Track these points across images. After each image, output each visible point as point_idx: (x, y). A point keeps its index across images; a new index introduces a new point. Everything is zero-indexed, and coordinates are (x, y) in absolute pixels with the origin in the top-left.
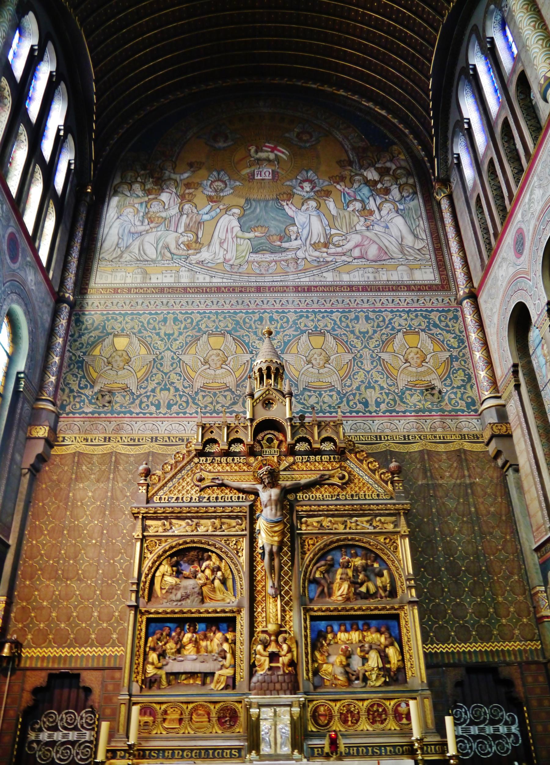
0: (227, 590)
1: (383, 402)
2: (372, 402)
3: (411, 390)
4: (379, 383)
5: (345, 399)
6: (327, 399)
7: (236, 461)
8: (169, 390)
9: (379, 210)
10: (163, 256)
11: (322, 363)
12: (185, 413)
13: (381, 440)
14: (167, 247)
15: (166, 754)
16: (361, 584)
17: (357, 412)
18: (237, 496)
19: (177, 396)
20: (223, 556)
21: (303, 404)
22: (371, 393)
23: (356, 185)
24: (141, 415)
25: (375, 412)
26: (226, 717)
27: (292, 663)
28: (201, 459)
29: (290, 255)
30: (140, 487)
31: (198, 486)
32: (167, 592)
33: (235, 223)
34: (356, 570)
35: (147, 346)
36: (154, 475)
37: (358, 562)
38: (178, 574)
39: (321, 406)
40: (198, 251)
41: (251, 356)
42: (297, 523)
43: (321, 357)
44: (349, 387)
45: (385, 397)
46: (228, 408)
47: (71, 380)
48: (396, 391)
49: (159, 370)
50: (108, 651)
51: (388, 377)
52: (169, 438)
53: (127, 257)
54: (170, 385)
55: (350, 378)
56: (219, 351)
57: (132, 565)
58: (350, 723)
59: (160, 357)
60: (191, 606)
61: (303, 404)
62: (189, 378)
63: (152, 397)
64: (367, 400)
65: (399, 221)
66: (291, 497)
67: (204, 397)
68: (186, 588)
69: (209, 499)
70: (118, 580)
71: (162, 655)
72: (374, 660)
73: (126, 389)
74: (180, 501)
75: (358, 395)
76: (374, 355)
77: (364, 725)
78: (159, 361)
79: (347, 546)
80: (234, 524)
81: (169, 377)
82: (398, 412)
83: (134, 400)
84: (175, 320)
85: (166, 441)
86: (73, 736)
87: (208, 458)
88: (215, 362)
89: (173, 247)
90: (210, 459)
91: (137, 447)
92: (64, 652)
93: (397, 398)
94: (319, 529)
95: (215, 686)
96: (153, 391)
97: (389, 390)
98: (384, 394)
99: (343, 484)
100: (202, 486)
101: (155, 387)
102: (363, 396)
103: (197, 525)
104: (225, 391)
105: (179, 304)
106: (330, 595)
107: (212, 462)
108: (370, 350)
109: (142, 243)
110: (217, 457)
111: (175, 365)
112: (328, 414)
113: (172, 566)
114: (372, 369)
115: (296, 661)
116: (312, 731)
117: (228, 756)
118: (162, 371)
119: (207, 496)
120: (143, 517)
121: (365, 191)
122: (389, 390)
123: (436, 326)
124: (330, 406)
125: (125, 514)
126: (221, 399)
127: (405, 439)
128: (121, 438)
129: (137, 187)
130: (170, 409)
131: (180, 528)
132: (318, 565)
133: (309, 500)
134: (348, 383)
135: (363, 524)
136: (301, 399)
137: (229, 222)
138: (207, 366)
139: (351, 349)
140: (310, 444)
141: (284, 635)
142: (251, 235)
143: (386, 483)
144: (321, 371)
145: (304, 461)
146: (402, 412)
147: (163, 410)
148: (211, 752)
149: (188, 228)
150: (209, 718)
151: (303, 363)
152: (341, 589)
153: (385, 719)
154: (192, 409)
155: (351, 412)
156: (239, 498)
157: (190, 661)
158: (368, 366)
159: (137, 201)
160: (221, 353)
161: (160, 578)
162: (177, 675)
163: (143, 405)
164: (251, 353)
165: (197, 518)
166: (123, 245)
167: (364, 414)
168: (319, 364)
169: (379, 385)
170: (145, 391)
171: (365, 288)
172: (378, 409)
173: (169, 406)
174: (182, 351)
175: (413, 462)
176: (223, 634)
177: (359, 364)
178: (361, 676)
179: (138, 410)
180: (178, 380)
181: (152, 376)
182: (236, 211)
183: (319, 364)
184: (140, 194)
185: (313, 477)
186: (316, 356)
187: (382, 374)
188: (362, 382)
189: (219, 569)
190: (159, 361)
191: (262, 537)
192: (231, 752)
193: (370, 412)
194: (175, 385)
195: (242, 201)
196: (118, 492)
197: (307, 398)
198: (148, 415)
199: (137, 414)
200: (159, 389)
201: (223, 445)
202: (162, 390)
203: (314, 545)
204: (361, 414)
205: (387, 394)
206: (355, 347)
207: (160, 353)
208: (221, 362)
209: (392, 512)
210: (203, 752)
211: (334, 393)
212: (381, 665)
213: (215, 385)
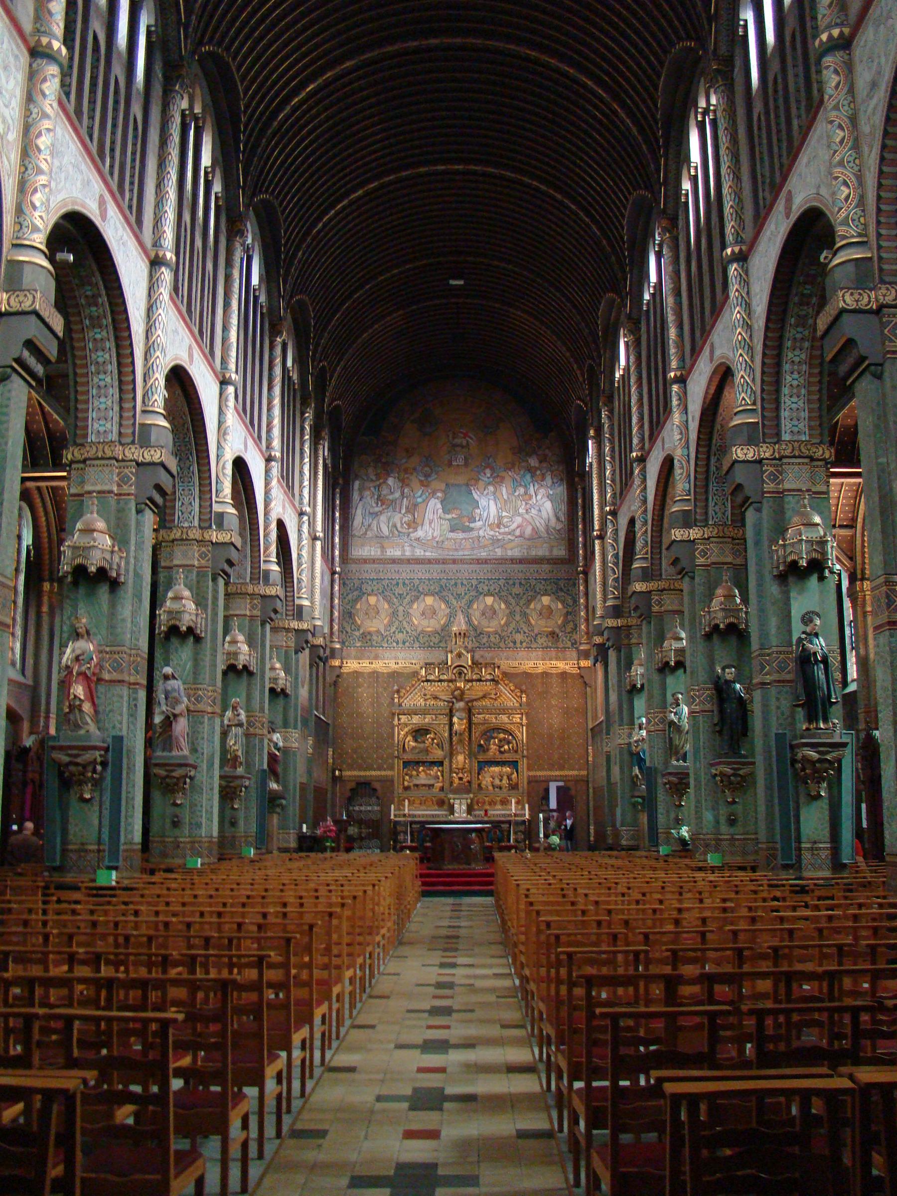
2: (518, 642)
10: (391, 532)
14: (395, 526)
29: (475, 533)
33: (439, 506)
35: (389, 602)
37: (502, 736)
38: (416, 741)
47: (345, 625)
50: (383, 773)
53: (370, 534)
60: (423, 757)
65: (548, 505)
71: (411, 776)
72: (505, 781)
73: (378, 632)
77: (499, 807)
79: (497, 729)
84: (404, 584)
86: (369, 808)
89: (399, 525)
92: (362, 773)
95: (435, 790)
105: (405, 572)
106: (488, 750)
109: (378, 523)
123: (561, 590)
129: (370, 470)
131: (416, 719)
135: (504, 718)
137: (434, 505)
142: (449, 516)
147: (400, 645)
149: (408, 510)
157: (423, 779)
158: (518, 617)
159: (371, 485)
162: (417, 786)
166: (366, 523)
173: (404, 643)
182: (439, 494)
185: (481, 694)
195: (443, 486)
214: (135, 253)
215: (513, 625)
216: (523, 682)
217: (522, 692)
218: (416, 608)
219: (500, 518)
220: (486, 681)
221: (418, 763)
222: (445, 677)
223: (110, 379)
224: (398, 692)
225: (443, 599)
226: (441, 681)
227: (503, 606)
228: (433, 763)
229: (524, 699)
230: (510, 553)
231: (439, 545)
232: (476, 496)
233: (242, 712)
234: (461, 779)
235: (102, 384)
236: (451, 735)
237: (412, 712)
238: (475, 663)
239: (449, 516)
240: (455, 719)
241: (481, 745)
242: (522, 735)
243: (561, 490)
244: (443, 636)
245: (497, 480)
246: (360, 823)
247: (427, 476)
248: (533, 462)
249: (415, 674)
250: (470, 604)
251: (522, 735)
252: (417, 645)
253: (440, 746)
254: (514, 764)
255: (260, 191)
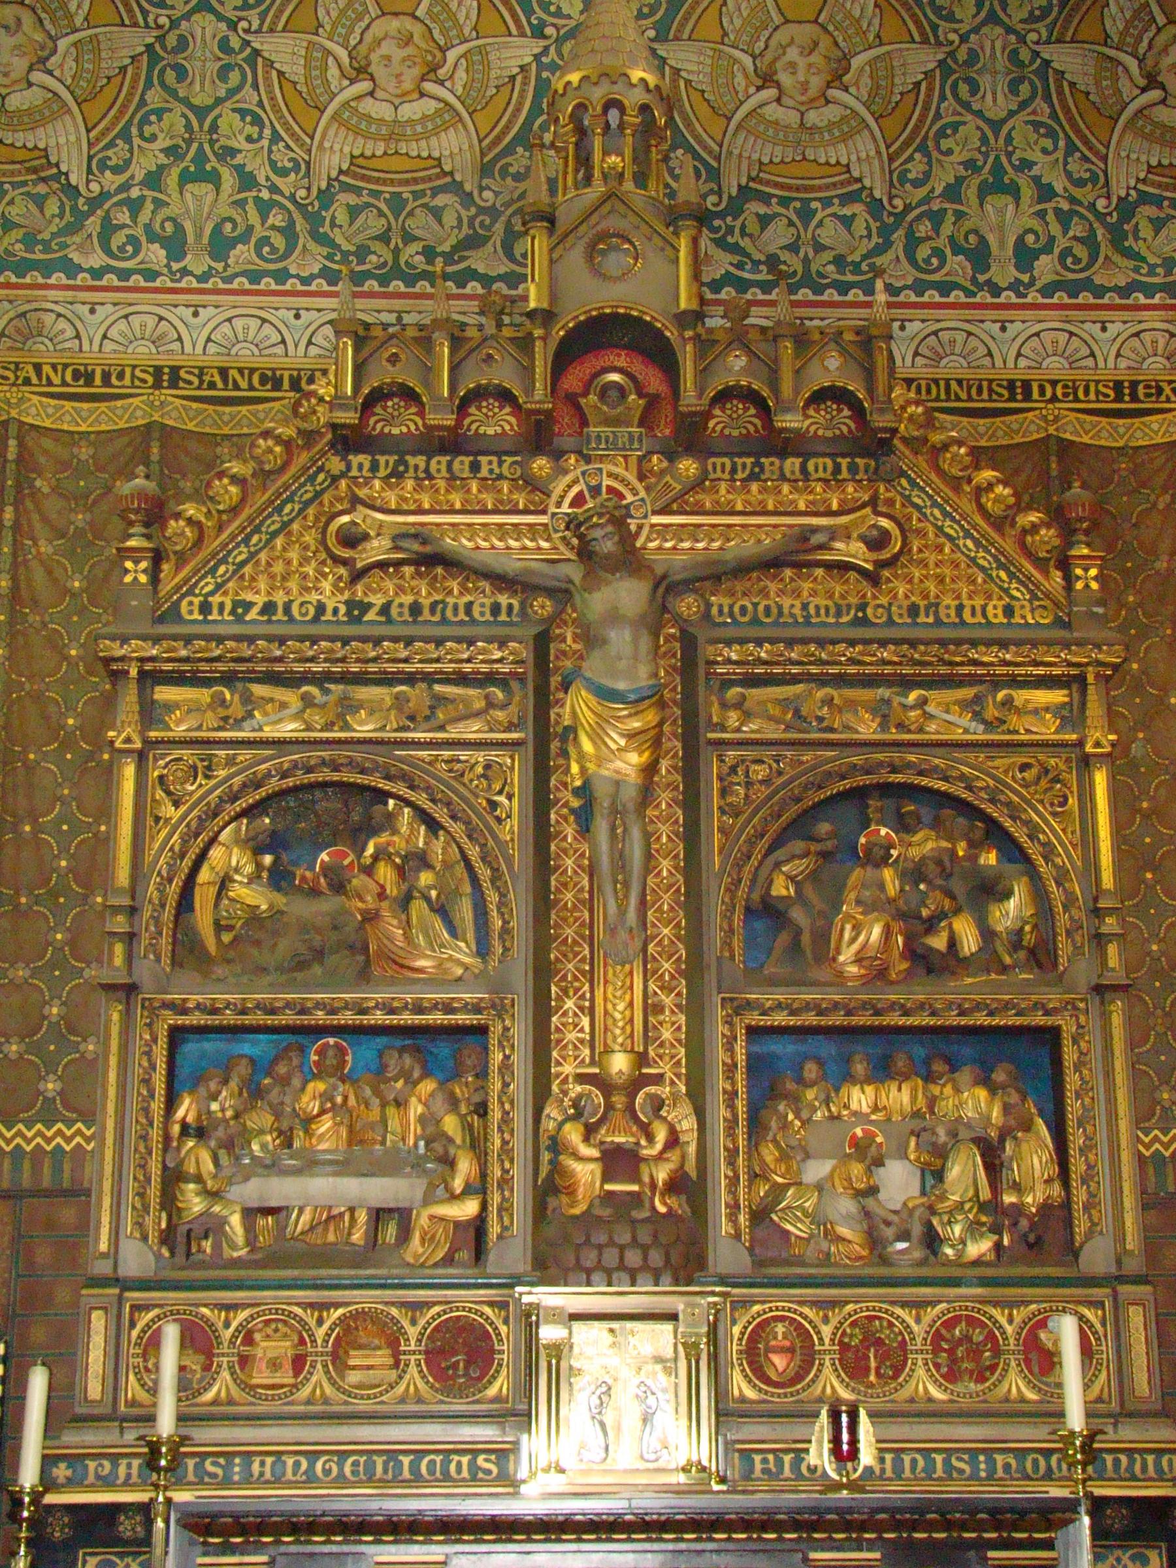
0: (453, 932)
1: (1048, 249)
2: (1002, 250)
3: (1158, 201)
4: (1035, 171)
5: (899, 236)
6: (830, 233)
7: (484, 472)
8: (214, 179)
11: (816, 83)
12: (282, 276)
13: (1027, 397)
15: (256, 1467)
16: (930, 926)
17: (945, 288)
18: (488, 602)
19: (250, 207)
20: (440, 814)
21: (735, 249)
22: (1001, 212)
24: (111, 279)
25: (1015, 286)
26: (454, 1353)
28: (356, 459)
30: (129, 565)
31: (344, 562)
32: (235, 939)
34: (915, 874)
36: (177, 516)
37: (925, 844)
38: (279, 878)
39: (806, 261)
41: (537, 46)
42: (709, 704)
43: (815, 58)
44: (917, 184)
45: (1055, 228)
46: (449, 258)
48: (1101, 204)
49: (174, 93)
50: (31, 1136)
51: (1071, 148)
52: (223, 372)
54: (221, 158)
55: (922, 148)
56: (408, 24)
57: (106, 842)
58: (872, 1378)
59: (172, 40)
61: (735, 249)
62: (293, 135)
63: (149, 206)
64: (983, 240)
66: (687, 606)
67: (354, 212)
68: (304, 927)
69: (385, 610)
70: (54, 894)
74: (280, 615)
75: (950, 218)
76: (1025, 55)
78: (170, 59)
80: (479, 704)
81: (214, 128)
82: (1099, 291)
83: (80, 218)
85: (212, 386)
87: (382, 459)
88: (396, 67)
90: (386, 461)
91: (103, 406)
93: (1100, 232)
94: (788, 728)
96: (154, 180)
97: (1073, 200)
98: (1050, 217)
99: (881, 564)
100: (359, 565)
101: (161, 168)
102: (968, 225)
103: (348, 706)
104: (435, 192)
107: (395, 473)
108: (1009, 30)
110: (414, 454)
111: (234, 77)
112: (831, 295)
113: (258, 851)
114: (1011, 114)
115: (693, 1175)
116: (743, 1399)
117: (465, 1474)
118: (186, 101)
119: (378, 600)
120: (141, 672)
122: (1073, 200)
124: (839, 261)
125: (66, 658)
126: (420, 223)
127: (1119, 398)
128: (38, 368)
130: (225, 258)
132: (780, 854)
133: (755, 621)
134: (916, 170)
135: (946, 716)
136: (730, 230)
138: (365, 86)
139: (935, 28)
140: (765, 412)
141: (652, 1089)
143: (1041, 564)
144: (812, 117)
145: (740, 475)
146: (1117, 289)
147: (198, 262)
148: (406, 1460)
150: (396, 1354)
151: (740, 79)
152: (861, 937)
153: (993, 1368)
154: (309, 260)
155: (919, 287)
156: (496, 609)
158: (995, 100)
160: (417, 30)
161: (213, 891)
163: (118, 239)
164: (538, 32)
165: (345, 678)
167: (970, 294)
168: (805, 87)
169: (1036, 180)
170: (121, 179)
172: (1026, 278)
173: (220, 246)
174: (263, 17)
175: (1144, 485)
176: (442, 1084)
177: (963, 89)
178: (917, 1230)
179: (97, 259)
180: (249, 139)
181: (145, 121)
183: (805, 87)
186: (793, 54)
187: (1051, 134)
188: (969, 164)
189: (422, 860)
190: (170, 59)
191: (582, 756)
192: (472, 1464)
193: (996, 290)
194: (239, 159)
196: (39, 575)
197: (753, 227)
198: (137, 280)
199: (97, 274)
200: (175, 172)
201: (436, 409)
202: (186, 178)
203: (765, 782)
204: (956, 296)
205: (1064, 219)
206: (951, 18)
207: (174, 24)
208: (417, 71)
209: (1057, 671)
210: (379, 1461)
211: (858, 208)
212: (985, 1194)
213: (395, 163)
215: (964, 144)
229: (1088, 578)
241: (768, 911)
252: (309, 260)
254: (1028, 1057)
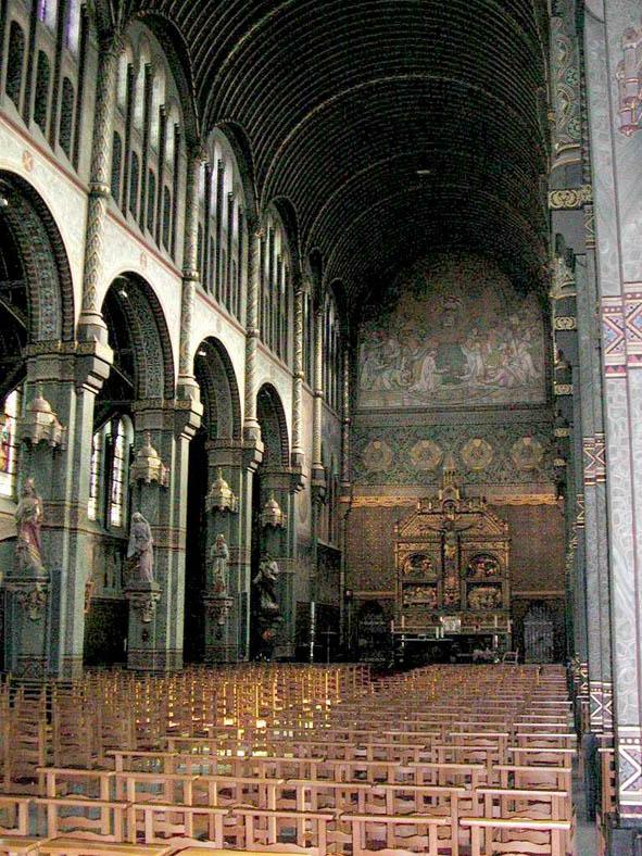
9: (517, 349)
10: (393, 386)
14: (395, 381)
23: (505, 329)
27: (459, 601)
40: (413, 384)
53: (374, 388)
72: (490, 600)
73: (383, 472)
79: (485, 555)
89: (399, 380)
105: (405, 420)
121: (510, 334)
131: (413, 547)
135: (489, 546)
137: (429, 362)
142: (442, 371)
154: (415, 482)
158: (502, 456)
171: (505, 408)
184: (377, 340)
214: (68, 189)
216: (506, 512)
217: (504, 522)
218: (415, 451)
219: (486, 371)
220: (473, 513)
221: (416, 585)
222: (439, 510)
223: (53, 291)
224: (398, 523)
225: (438, 442)
226: (433, 513)
227: (490, 448)
228: (427, 585)
230: (494, 401)
231: (434, 396)
232: (464, 352)
233: (225, 545)
234: (452, 598)
235: (48, 294)
236: (443, 560)
237: (410, 540)
238: (462, 496)
239: (442, 371)
240: (446, 547)
241: (469, 569)
242: (505, 560)
243: (540, 343)
244: (437, 473)
245: (483, 337)
246: (367, 635)
247: (422, 337)
248: (514, 320)
249: (414, 507)
250: (461, 445)
251: (505, 560)
253: (435, 569)
254: (498, 585)
255: (221, 117)
